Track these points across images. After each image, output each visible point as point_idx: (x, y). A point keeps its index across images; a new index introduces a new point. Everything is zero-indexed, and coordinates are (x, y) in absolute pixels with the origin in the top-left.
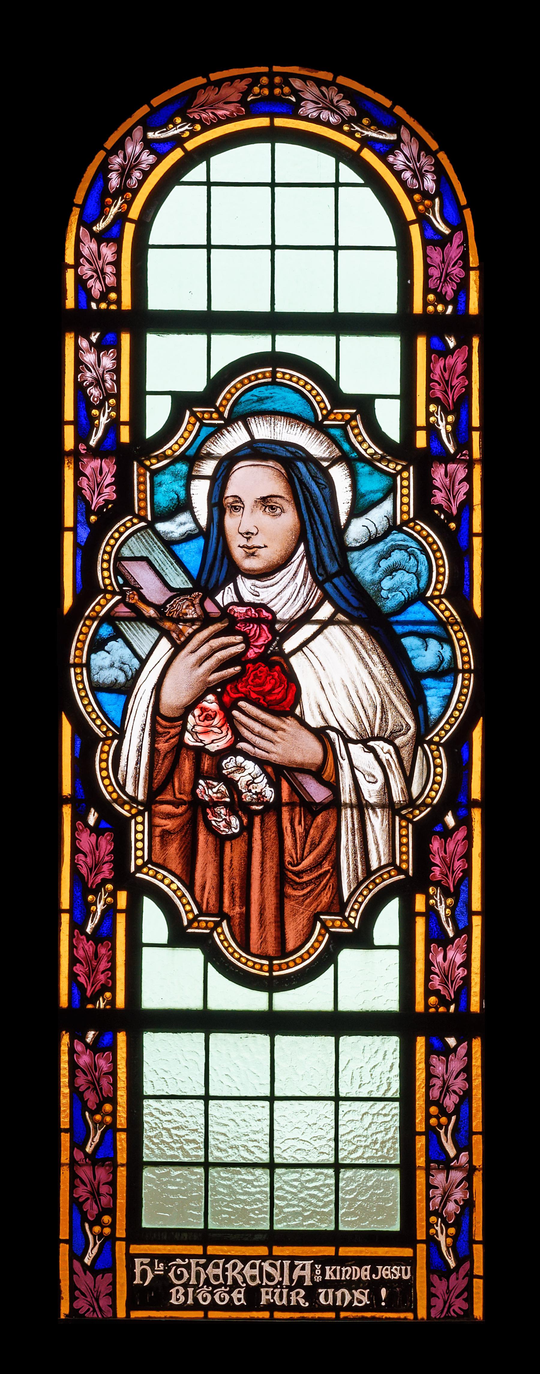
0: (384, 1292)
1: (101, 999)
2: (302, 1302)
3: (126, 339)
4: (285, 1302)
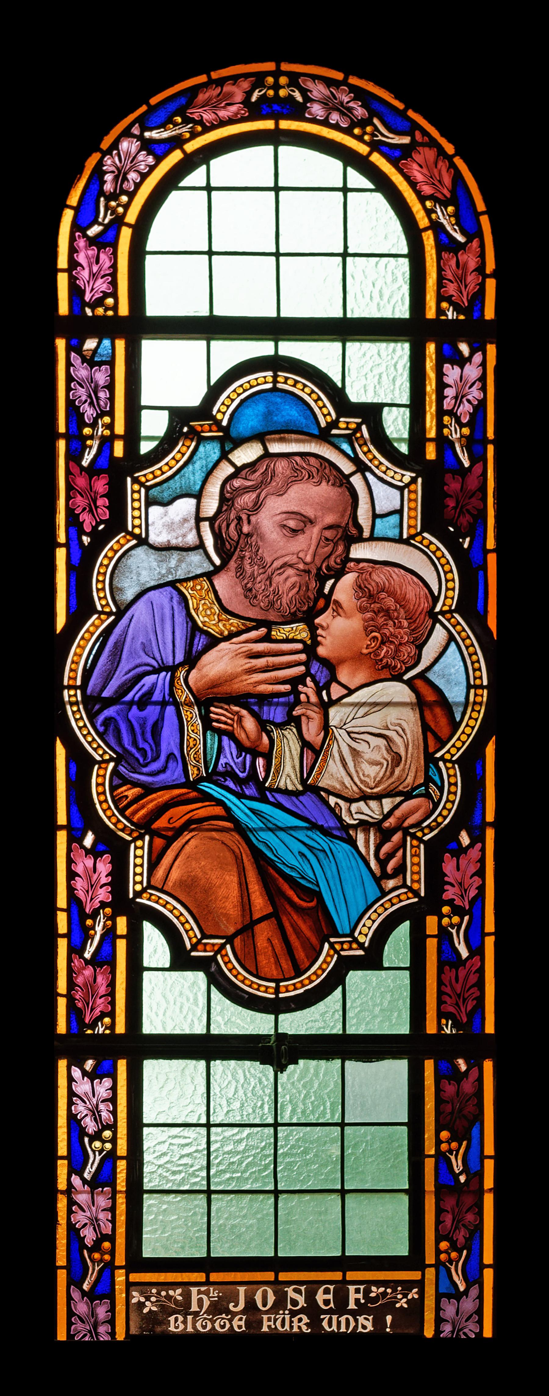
0: (389, 1318)
1: (100, 1024)
2: (304, 1328)
3: (122, 1065)
4: (287, 1327)
